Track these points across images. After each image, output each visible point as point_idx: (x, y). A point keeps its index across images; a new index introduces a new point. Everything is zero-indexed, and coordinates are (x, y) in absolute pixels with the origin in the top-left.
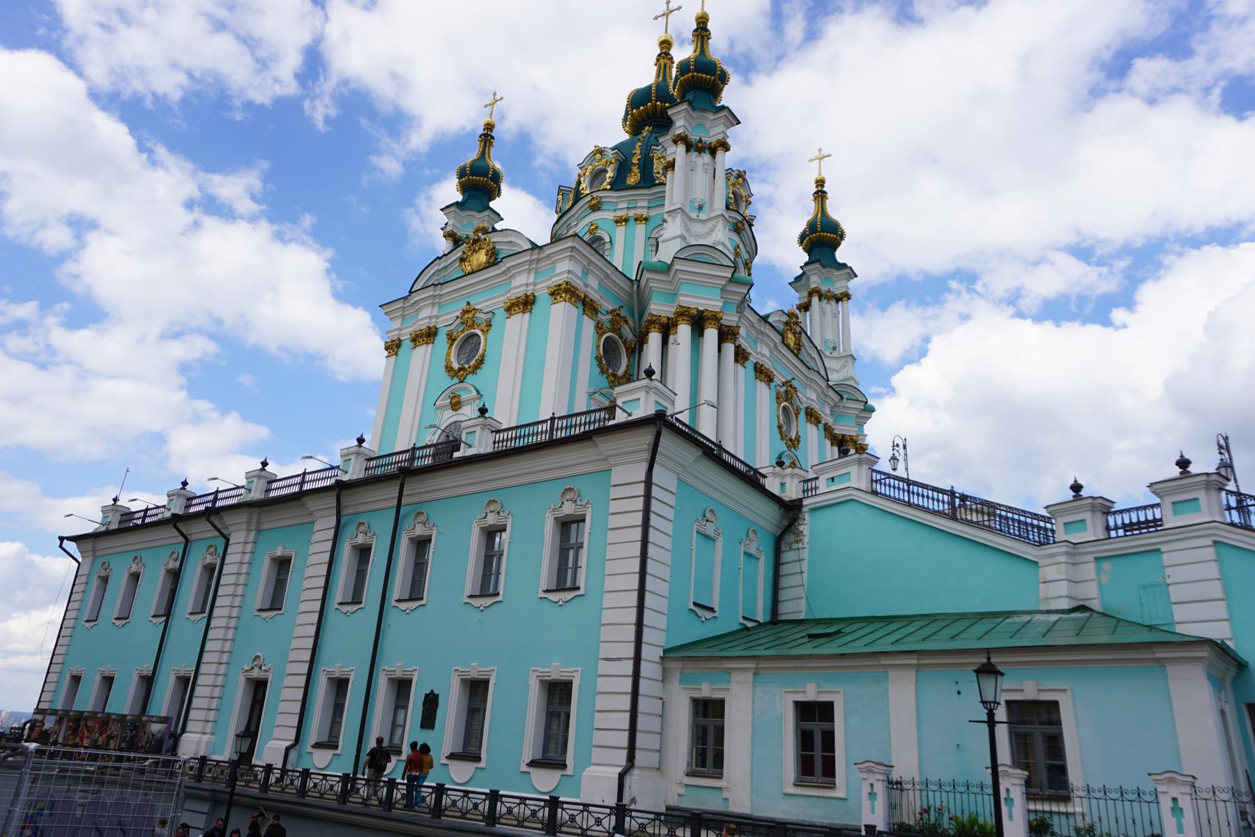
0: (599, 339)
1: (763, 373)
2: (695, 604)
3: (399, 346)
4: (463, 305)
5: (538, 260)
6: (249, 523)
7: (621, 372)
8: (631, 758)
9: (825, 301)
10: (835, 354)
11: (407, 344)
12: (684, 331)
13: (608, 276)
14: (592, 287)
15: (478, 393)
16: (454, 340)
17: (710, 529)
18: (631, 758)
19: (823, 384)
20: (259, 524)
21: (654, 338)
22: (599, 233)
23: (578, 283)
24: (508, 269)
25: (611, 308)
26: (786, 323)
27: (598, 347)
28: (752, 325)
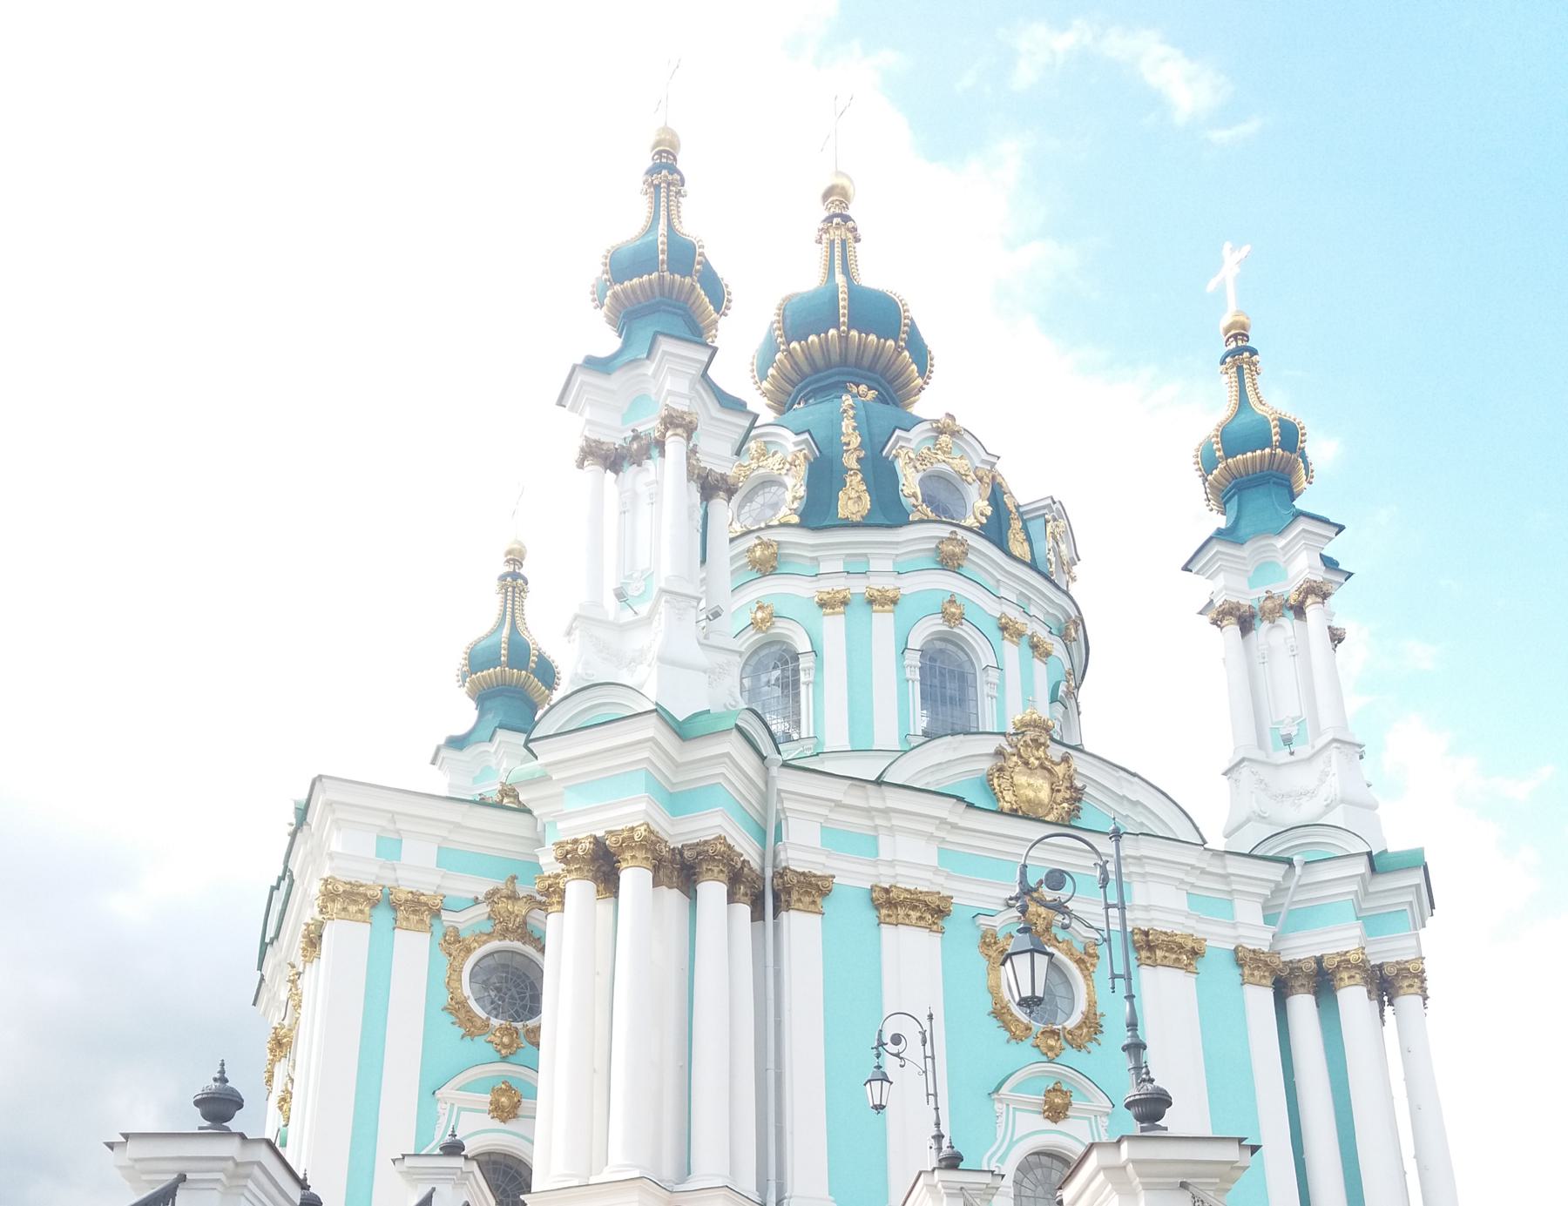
1: (891, 904)
9: (1266, 625)
10: (1303, 750)
13: (458, 826)
19: (1190, 856)
23: (368, 873)
25: (482, 889)
26: (999, 753)
27: (452, 981)
28: (839, 805)
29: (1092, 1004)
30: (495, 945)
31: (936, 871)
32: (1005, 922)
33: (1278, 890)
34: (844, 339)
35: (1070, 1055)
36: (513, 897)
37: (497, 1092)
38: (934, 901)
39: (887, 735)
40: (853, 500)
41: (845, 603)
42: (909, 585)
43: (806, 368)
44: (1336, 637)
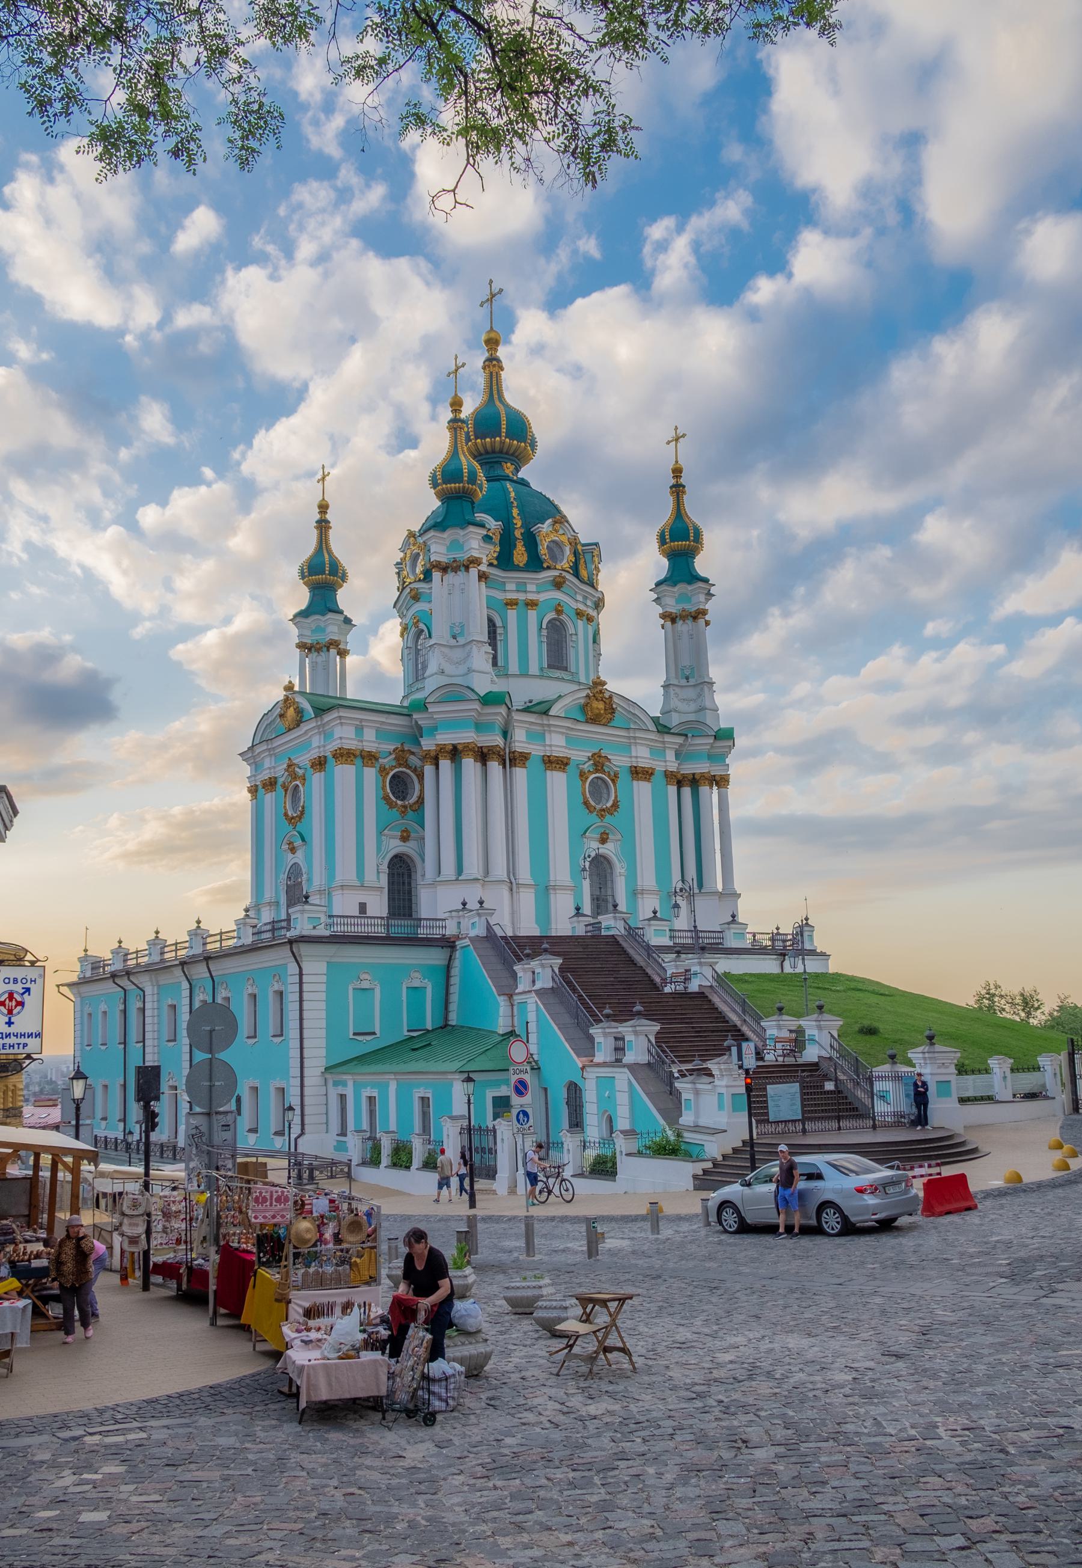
0: (384, 782)
2: (355, 1034)
3: (256, 791)
4: (287, 761)
5: (324, 725)
6: (151, 981)
7: (412, 801)
8: (303, 1129)
9: (681, 622)
10: (692, 681)
11: (261, 791)
12: (445, 764)
14: (370, 741)
15: (303, 840)
16: (286, 791)
17: (365, 985)
18: (303, 1129)
20: (157, 981)
21: (429, 769)
22: (422, 626)
23: (352, 744)
24: (306, 732)
26: (588, 696)
27: (384, 788)
29: (616, 797)
30: (397, 770)
31: (565, 748)
32: (588, 766)
33: (681, 745)
34: (502, 443)
35: (608, 817)
36: (403, 751)
37: (403, 831)
38: (565, 761)
39: (534, 669)
40: (520, 555)
41: (516, 604)
42: (542, 597)
43: (482, 451)
44: (707, 623)
